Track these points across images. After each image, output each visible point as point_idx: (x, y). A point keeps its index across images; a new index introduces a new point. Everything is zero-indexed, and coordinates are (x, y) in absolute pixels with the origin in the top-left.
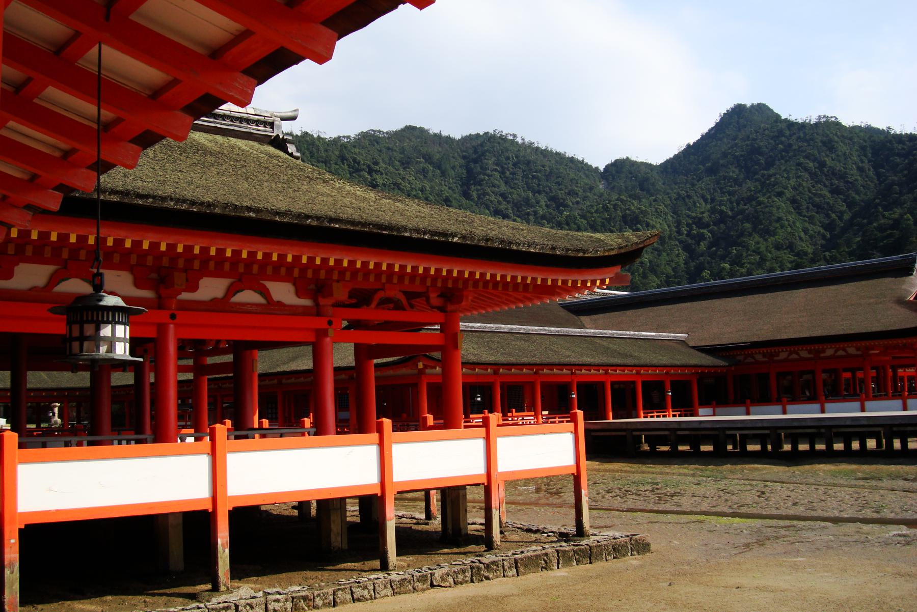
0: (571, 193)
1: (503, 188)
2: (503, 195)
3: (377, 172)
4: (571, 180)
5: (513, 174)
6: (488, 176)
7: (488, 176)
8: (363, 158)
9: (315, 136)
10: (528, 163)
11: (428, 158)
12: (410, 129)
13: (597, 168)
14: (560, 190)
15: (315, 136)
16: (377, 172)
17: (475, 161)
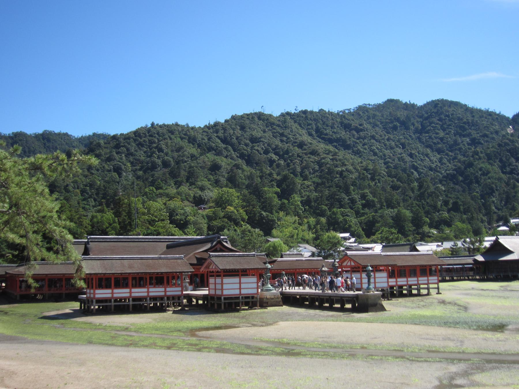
0: (485, 136)
1: (442, 134)
2: (442, 139)
3: (361, 130)
4: (485, 127)
5: (450, 125)
6: (433, 127)
7: (433, 127)
8: (355, 123)
9: (327, 111)
10: (459, 119)
11: (398, 120)
12: (390, 102)
13: (508, 118)
14: (478, 133)
15: (327, 111)
16: (361, 130)
17: (426, 119)
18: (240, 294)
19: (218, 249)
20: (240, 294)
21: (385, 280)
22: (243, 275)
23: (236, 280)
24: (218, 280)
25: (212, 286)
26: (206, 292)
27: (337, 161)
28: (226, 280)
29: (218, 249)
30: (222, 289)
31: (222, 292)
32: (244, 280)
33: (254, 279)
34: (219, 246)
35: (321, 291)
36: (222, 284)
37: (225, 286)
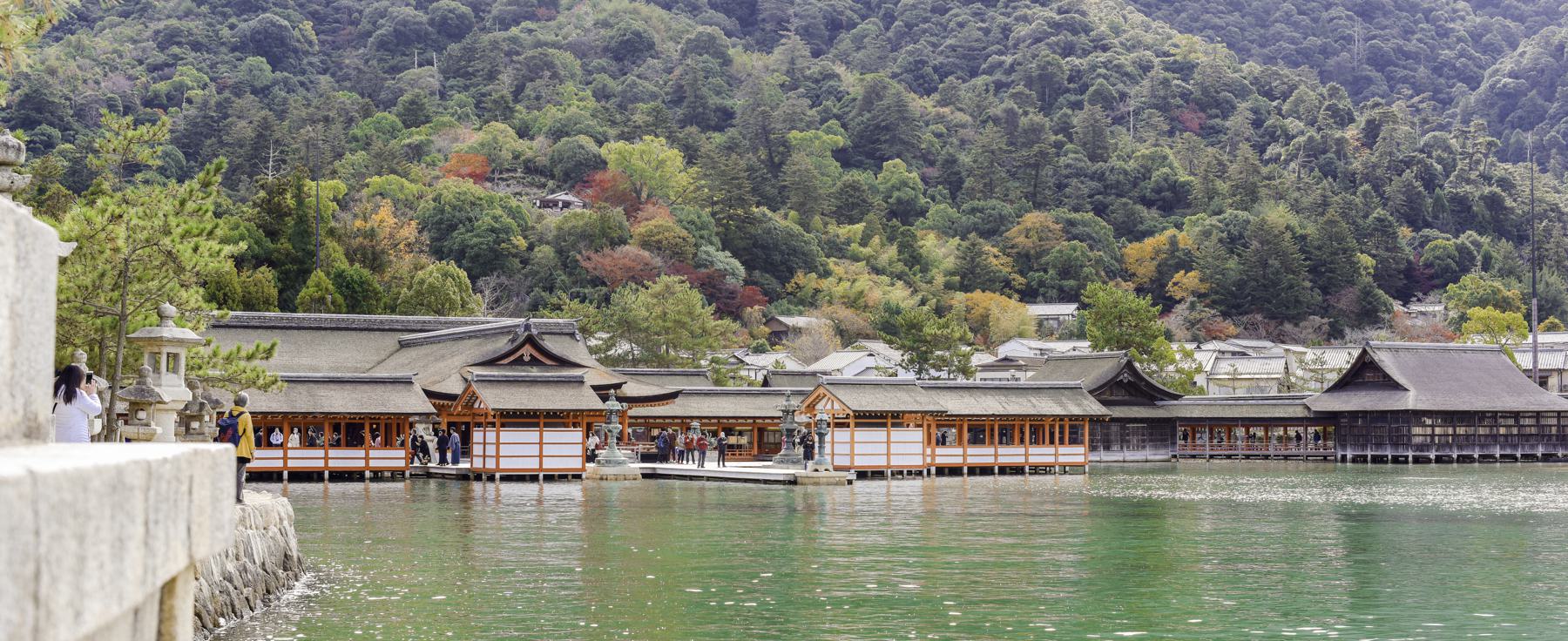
18: (541, 469)
19: (527, 359)
20: (541, 469)
21: (919, 448)
22: (546, 425)
23: (532, 435)
24: (491, 436)
25: (477, 450)
26: (468, 466)
27: (1075, 32)
28: (507, 435)
29: (527, 359)
30: (498, 457)
31: (498, 463)
32: (551, 435)
33: (577, 435)
34: (527, 351)
35: (695, 467)
36: (498, 444)
37: (504, 450)
